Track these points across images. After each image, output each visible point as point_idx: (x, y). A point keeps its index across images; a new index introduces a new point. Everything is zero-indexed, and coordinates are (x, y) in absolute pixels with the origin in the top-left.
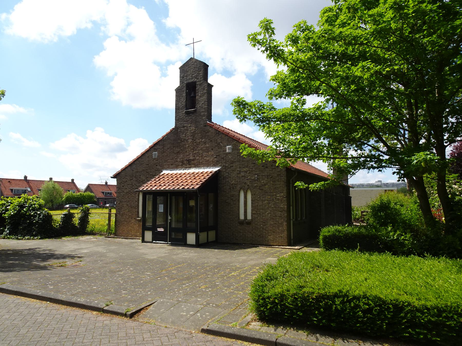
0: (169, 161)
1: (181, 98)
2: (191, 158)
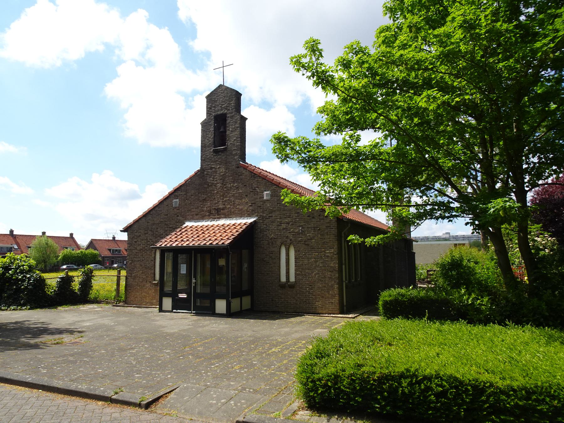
0: (193, 210)
2: (221, 207)
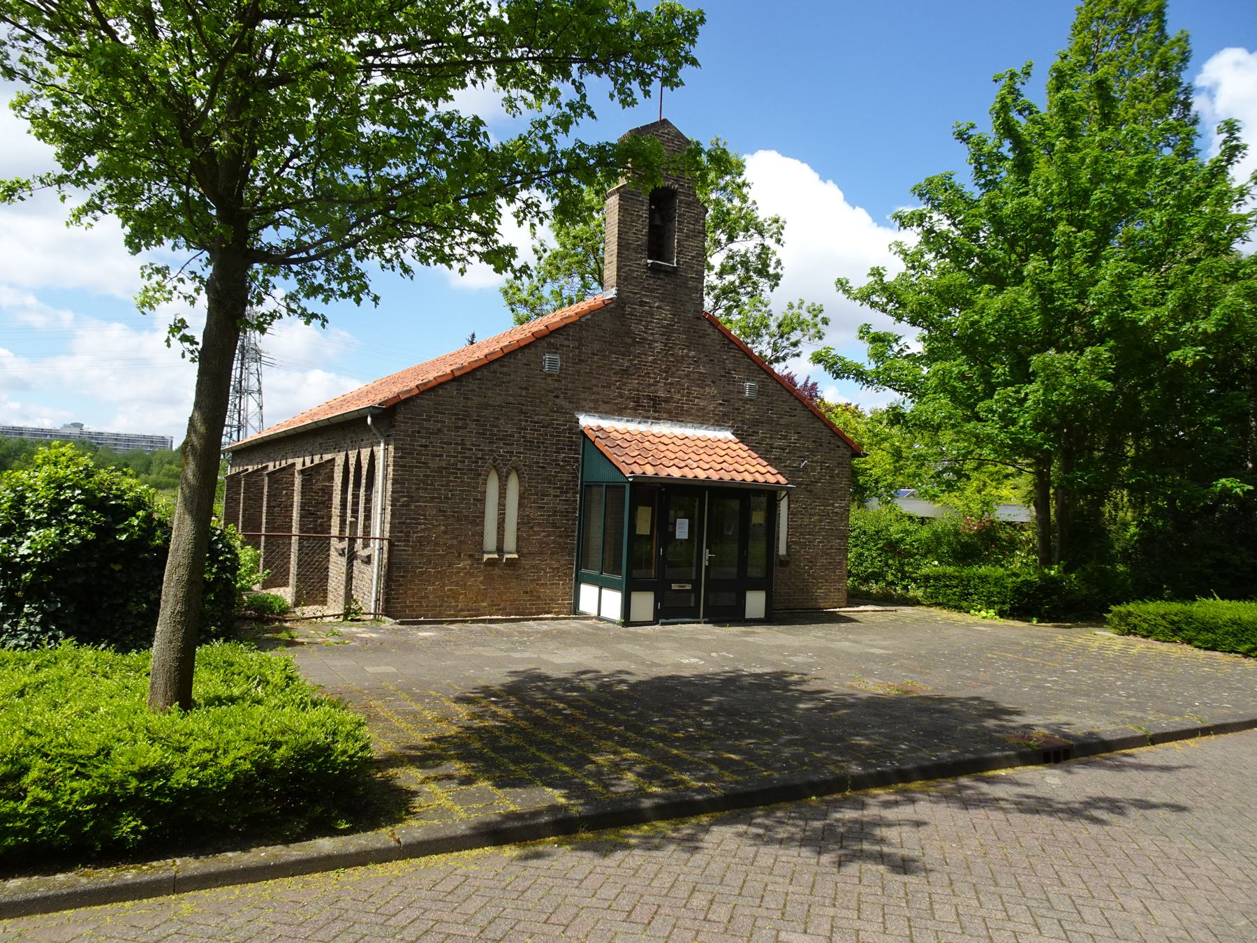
0: (595, 389)
1: (635, 218)
2: (661, 394)
